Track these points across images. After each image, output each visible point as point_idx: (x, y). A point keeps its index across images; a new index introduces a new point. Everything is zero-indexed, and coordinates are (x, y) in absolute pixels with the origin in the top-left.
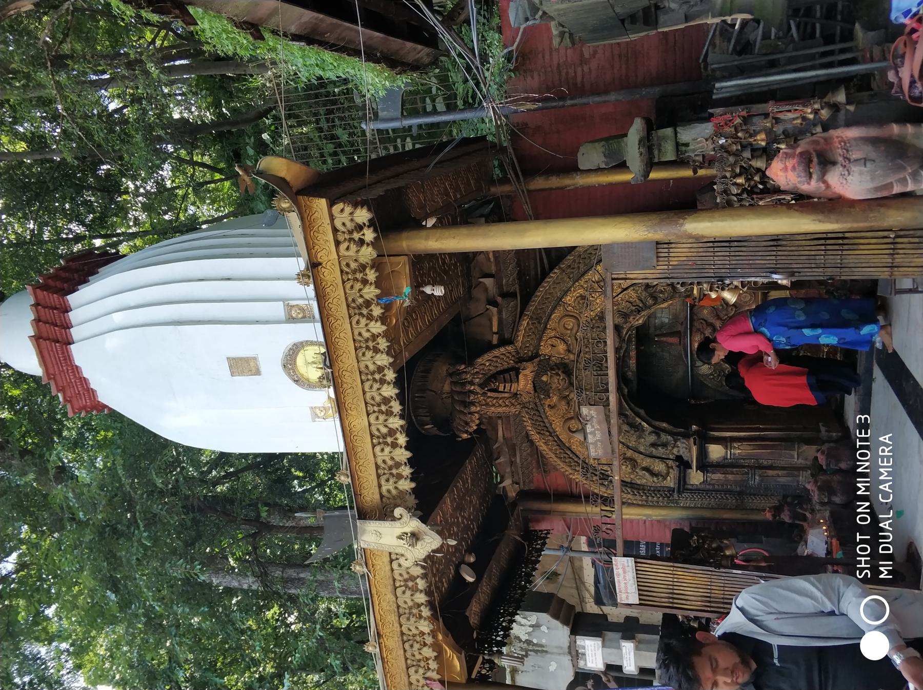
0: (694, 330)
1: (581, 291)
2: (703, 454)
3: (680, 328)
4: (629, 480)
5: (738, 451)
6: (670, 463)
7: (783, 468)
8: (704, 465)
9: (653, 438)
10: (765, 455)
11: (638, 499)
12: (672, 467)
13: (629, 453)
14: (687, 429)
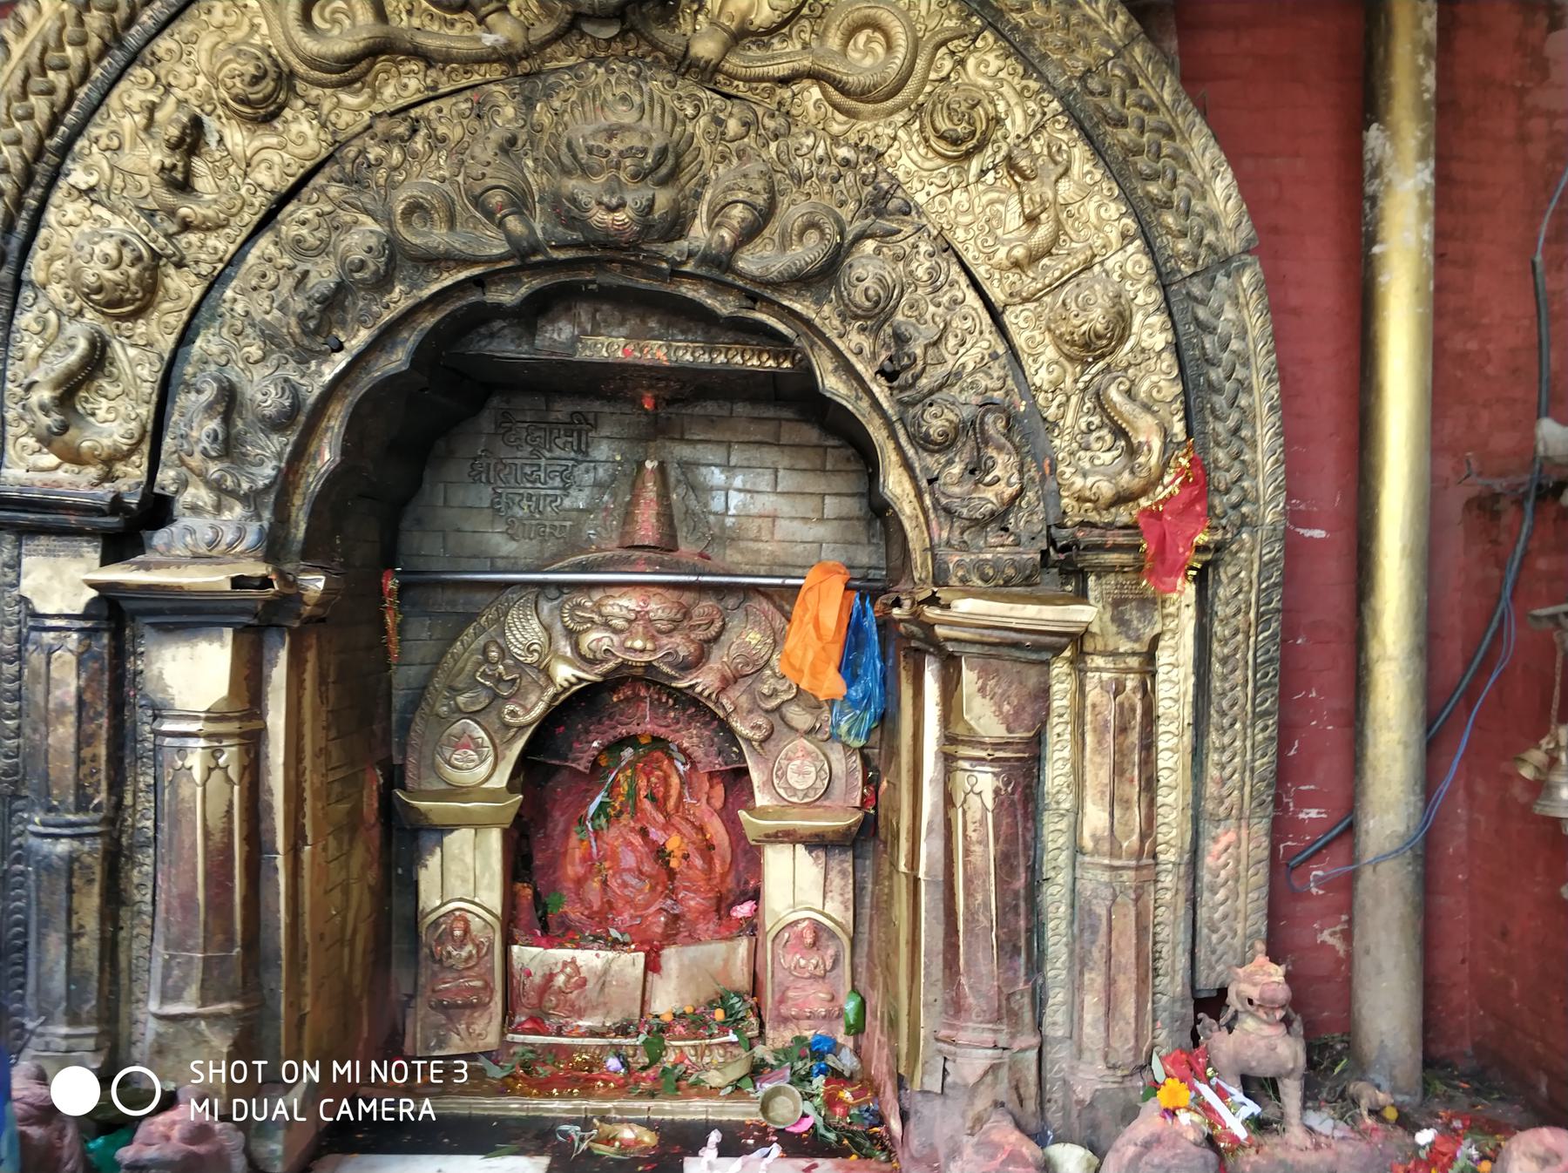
1: (1016, 124)
2: (186, 615)
4: (36, 268)
5: (197, 777)
6: (133, 474)
7: (110, 948)
8: (117, 620)
9: (263, 390)
13: (182, 287)
14: (306, 554)
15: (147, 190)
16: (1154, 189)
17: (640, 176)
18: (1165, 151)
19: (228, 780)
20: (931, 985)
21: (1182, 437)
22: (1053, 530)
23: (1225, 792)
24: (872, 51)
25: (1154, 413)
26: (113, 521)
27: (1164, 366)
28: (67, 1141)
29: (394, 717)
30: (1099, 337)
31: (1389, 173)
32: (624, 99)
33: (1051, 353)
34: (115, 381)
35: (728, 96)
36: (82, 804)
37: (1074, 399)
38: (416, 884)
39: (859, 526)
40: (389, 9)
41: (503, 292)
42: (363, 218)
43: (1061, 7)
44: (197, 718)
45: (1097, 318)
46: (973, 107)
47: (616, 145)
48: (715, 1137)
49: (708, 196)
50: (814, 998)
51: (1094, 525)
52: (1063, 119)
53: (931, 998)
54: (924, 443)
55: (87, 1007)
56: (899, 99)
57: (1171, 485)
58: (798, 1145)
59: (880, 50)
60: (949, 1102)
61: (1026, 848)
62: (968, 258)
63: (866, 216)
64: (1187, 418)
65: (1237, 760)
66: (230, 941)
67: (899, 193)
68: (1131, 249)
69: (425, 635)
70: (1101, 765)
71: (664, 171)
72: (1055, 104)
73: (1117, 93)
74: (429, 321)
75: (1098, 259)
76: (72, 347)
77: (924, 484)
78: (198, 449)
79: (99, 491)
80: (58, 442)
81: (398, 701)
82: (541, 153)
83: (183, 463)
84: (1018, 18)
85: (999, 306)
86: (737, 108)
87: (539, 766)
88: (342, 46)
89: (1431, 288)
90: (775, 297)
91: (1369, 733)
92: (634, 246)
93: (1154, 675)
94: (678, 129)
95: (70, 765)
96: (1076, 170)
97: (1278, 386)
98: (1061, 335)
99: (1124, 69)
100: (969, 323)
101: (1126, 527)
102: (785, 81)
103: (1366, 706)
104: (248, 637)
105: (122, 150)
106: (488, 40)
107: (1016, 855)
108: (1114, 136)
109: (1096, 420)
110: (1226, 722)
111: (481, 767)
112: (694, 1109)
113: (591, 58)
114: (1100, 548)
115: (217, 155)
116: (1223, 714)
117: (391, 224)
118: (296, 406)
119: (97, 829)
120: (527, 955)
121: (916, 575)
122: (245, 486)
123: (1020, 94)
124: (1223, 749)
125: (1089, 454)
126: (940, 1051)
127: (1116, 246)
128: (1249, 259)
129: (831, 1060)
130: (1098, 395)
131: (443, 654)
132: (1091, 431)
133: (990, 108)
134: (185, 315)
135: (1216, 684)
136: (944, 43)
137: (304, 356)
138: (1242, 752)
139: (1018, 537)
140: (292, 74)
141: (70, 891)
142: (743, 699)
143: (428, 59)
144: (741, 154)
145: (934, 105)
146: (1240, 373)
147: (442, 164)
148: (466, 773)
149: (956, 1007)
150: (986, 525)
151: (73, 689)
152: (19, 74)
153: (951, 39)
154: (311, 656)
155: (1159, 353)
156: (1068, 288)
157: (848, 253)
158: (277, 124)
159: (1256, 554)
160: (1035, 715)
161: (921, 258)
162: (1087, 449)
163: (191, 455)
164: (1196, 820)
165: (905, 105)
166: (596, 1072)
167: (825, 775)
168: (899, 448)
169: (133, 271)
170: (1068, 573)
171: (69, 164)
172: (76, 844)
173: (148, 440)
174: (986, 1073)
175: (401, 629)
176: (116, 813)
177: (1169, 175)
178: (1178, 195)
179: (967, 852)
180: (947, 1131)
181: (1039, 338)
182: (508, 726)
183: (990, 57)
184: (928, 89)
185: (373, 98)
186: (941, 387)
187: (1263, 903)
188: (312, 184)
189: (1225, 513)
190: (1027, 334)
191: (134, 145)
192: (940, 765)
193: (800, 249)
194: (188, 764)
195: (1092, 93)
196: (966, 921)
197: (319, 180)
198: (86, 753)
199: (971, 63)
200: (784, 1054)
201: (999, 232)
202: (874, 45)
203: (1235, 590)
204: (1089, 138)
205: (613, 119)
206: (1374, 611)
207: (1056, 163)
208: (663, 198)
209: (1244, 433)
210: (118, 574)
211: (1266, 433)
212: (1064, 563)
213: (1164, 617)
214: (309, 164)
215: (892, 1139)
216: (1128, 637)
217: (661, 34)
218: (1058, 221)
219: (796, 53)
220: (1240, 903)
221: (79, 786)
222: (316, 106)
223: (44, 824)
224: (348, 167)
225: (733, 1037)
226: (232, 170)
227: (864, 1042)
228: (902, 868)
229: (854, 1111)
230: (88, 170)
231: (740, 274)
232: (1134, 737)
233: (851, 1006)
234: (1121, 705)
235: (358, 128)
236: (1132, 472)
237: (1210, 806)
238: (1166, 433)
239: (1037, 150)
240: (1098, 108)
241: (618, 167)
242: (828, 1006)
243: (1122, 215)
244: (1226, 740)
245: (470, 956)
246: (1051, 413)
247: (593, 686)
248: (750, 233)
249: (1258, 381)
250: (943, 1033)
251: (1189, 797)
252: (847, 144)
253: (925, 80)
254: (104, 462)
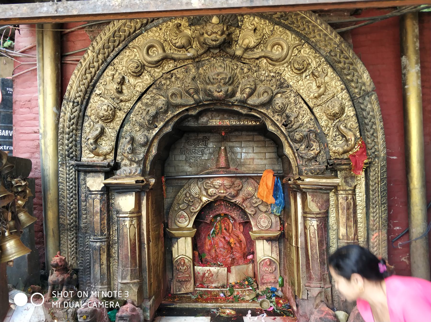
0: (233, 180)
1: (314, 65)
2: (124, 189)
3: (232, 168)
4: (88, 112)
6: (111, 157)
8: (108, 190)
9: (140, 137)
10: (123, 251)
11: (65, 122)
12: (105, 159)
13: (121, 115)
14: (149, 174)
15: (113, 93)
16: (348, 77)
17: (225, 84)
18: (351, 68)
19: (135, 227)
20: (303, 273)
21: (359, 136)
22: (328, 161)
23: (375, 223)
24: (278, 50)
25: (352, 131)
26: (108, 169)
27: (354, 120)
28: (104, 312)
29: (165, 211)
30: (337, 114)
31: (408, 68)
32: (220, 66)
33: (325, 118)
34: (106, 137)
35: (244, 63)
36: (102, 234)
37: (332, 129)
38: (172, 251)
39: (275, 160)
40: (166, 49)
41: (193, 112)
42: (161, 97)
43: (323, 36)
44: (127, 213)
45: (337, 109)
46: (303, 62)
47: (220, 77)
48: (249, 312)
49: (240, 87)
50: (271, 278)
51: (338, 159)
52: (325, 63)
53: (303, 276)
54: (295, 141)
55: (105, 281)
56: (285, 61)
57: (357, 148)
58: (271, 314)
59: (280, 50)
60: (309, 301)
61: (326, 239)
62: (304, 96)
63: (278, 88)
64: (360, 132)
65: (378, 215)
66: (136, 265)
67: (286, 83)
68: (344, 92)
69: (171, 191)
70: (343, 218)
71: (230, 82)
72: (323, 59)
73: (338, 55)
74: (176, 120)
75: (336, 95)
76: (97, 130)
77: (295, 151)
78: (126, 152)
79: (103, 162)
80: (94, 152)
81: (165, 207)
82: (201, 80)
83: (123, 155)
84: (313, 40)
85: (312, 107)
86: (246, 66)
88: (156, 59)
89: (421, 95)
90: (257, 109)
91: (412, 207)
92: (224, 100)
93: (355, 195)
94: (233, 72)
95: (99, 225)
96: (329, 74)
97: (382, 123)
98: (328, 114)
99: (340, 50)
100: (305, 112)
101: (346, 159)
102: (257, 59)
103: (410, 201)
104: (138, 194)
105: (107, 84)
106: (189, 55)
107: (323, 241)
108: (338, 65)
109: (337, 133)
110: (374, 206)
111: (186, 222)
112: (243, 306)
113: (212, 57)
114: (340, 164)
115: (128, 85)
116: (373, 204)
117: (168, 98)
118: (148, 141)
119: (105, 240)
120: (199, 269)
121: (294, 173)
122: (137, 159)
123: (314, 57)
124: (374, 213)
125: (336, 142)
126: (306, 289)
127: (340, 91)
128: (374, 92)
129: (276, 293)
130: (337, 127)
131: (176, 196)
132: (336, 136)
133: (307, 61)
134: (122, 121)
135: (371, 196)
136: (295, 47)
137: (149, 129)
138: (379, 214)
139: (320, 163)
140: (144, 65)
141: (100, 254)
142: (248, 204)
143: (175, 60)
144: (248, 76)
145: (294, 62)
146: (373, 120)
147: (178, 84)
148: (183, 224)
149: (310, 278)
150: (312, 160)
151: (99, 208)
152: (84, 69)
153: (297, 46)
154: (150, 198)
155: (352, 117)
156: (329, 102)
157: (274, 97)
158: (141, 77)
159: (379, 164)
160: (326, 206)
161: (292, 97)
162: (335, 141)
163: (125, 153)
164: (368, 230)
165: (287, 62)
166: (218, 297)
167: (270, 223)
168: (288, 142)
169: (111, 112)
170: (332, 171)
171: (95, 89)
172: (101, 243)
173: (114, 150)
174: (319, 294)
175: (166, 190)
176: (109, 237)
177: (352, 74)
178: (355, 78)
179: (311, 240)
180: (309, 308)
181: (322, 115)
182: (192, 212)
183: (307, 49)
184: (292, 58)
185: (162, 69)
186: (298, 128)
187: (386, 251)
188: (149, 90)
189: (371, 154)
190: (319, 114)
191: (109, 83)
192: (303, 219)
193: (263, 98)
194: (126, 224)
195: (332, 56)
196: (311, 257)
197: (151, 89)
198: (102, 222)
199: (302, 51)
200: (264, 292)
201: (311, 90)
202: (279, 49)
203: (374, 173)
204: (332, 66)
205: (218, 71)
206: (411, 176)
207: (324, 73)
208: (230, 88)
209: (374, 135)
210: (109, 181)
211: (380, 134)
212: (332, 169)
213: (357, 180)
214: (148, 85)
215: (294, 311)
216: (349, 186)
217: (228, 50)
218: (326, 87)
219: (260, 52)
220: (380, 251)
221: (101, 230)
222: (150, 72)
223: (94, 239)
224: (157, 86)
225: (251, 288)
226: (131, 88)
227: (284, 289)
228: (294, 245)
229: (283, 305)
230: (99, 90)
231: (248, 104)
232: (351, 210)
233: (280, 280)
234: (348, 203)
235: (159, 77)
236: (347, 146)
237: (371, 227)
238: (355, 135)
239: (319, 70)
240: (334, 59)
241: (220, 82)
242: (274, 280)
243: (341, 84)
244: (374, 210)
245: (186, 269)
246: (326, 132)
247: (211, 202)
248: (250, 95)
249: (377, 122)
250: (307, 284)
251: (366, 225)
252: (273, 72)
253: (291, 56)
254: (104, 155)
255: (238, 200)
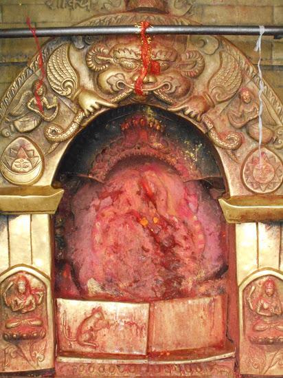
87: (71, 172)
182: (51, 142)
245: (31, 303)
255: (192, 109)
